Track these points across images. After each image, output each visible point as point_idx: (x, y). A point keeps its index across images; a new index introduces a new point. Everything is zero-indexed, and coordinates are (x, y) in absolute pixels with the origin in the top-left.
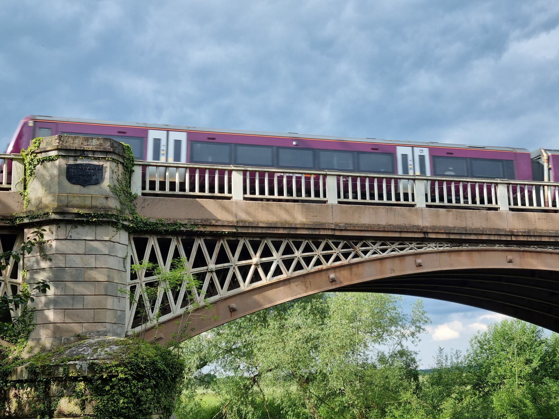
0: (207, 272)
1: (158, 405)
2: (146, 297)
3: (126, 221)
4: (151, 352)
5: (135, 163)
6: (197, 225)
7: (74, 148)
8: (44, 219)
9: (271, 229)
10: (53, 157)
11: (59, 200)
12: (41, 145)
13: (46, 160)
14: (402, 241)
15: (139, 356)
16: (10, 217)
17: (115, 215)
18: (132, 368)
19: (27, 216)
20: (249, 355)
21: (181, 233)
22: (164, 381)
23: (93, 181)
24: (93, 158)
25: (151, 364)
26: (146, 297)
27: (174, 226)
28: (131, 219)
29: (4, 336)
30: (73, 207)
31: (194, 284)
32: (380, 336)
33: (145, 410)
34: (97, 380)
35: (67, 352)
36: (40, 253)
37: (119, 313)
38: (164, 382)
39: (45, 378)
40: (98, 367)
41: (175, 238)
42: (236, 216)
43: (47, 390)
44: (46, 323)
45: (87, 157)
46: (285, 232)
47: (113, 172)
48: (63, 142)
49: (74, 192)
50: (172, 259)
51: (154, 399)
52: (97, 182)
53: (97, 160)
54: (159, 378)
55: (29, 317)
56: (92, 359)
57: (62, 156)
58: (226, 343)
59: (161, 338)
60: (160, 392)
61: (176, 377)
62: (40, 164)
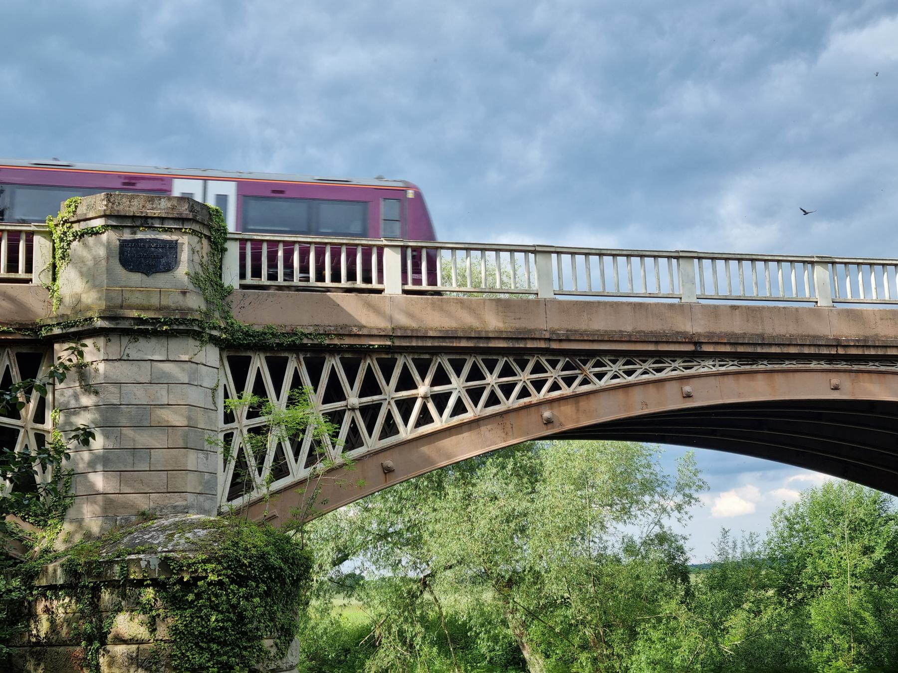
0: (346, 410)
1: (271, 624)
2: (249, 451)
3: (216, 329)
4: (259, 539)
5: (229, 236)
6: (329, 335)
7: (132, 214)
8: (86, 328)
9: (447, 340)
10: (97, 229)
11: (108, 298)
12: (78, 209)
13: (87, 233)
14: (659, 357)
15: (240, 545)
16: (32, 324)
17: (197, 320)
18: (229, 566)
19: (58, 324)
20: (416, 543)
22: (281, 585)
23: (161, 267)
25: (260, 559)
26: (249, 450)
27: (291, 337)
28: (223, 326)
29: (25, 515)
30: (131, 308)
31: (325, 429)
32: (625, 511)
33: (251, 631)
34: (174, 584)
35: (125, 540)
36: (80, 383)
37: (207, 476)
38: (281, 587)
39: (92, 582)
40: (175, 564)
41: (295, 356)
42: (391, 319)
43: (96, 600)
44: (92, 494)
46: (470, 344)
47: (193, 251)
48: (113, 204)
50: (290, 390)
51: (265, 614)
52: (169, 268)
53: (168, 233)
54: (273, 580)
55: (65, 484)
56: (165, 552)
57: (112, 226)
58: (378, 525)
60: (274, 603)
61: (299, 580)
62: (77, 240)
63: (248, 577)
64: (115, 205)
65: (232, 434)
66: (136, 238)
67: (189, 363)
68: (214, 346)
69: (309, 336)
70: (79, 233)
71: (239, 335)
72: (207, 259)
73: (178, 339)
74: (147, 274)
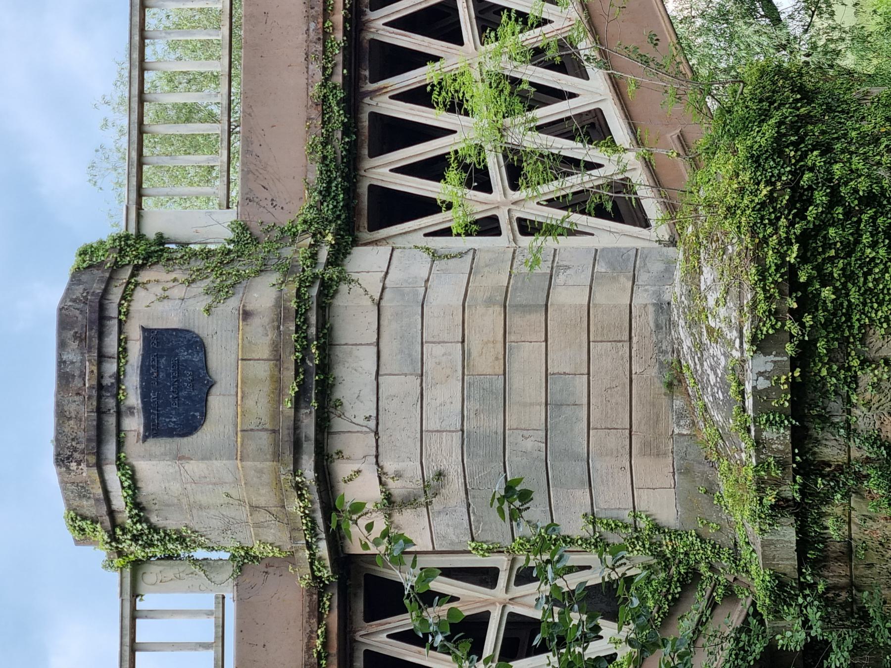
2: (553, 189)
3: (316, 254)
5: (132, 231)
6: (325, 33)
8: (316, 497)
10: (124, 478)
12: (88, 514)
15: (733, 204)
16: (311, 595)
17: (298, 290)
18: (771, 223)
19: (309, 546)
21: (352, 84)
22: (811, 124)
23: (196, 359)
24: (123, 361)
25: (760, 165)
26: (552, 188)
27: (330, 107)
28: (310, 240)
29: (667, 600)
34: (802, 325)
35: (718, 417)
37: (601, 268)
38: (814, 124)
39: (794, 477)
40: (764, 325)
41: (367, 100)
43: (828, 469)
45: (119, 378)
49: (230, 413)
50: (434, 108)
51: (865, 153)
54: (802, 140)
55: (612, 529)
56: (741, 343)
59: (682, 139)
60: (845, 136)
61: (801, 89)
63: (794, 186)
64: (78, 446)
65: (521, 222)
66: (140, 406)
67: (383, 303)
68: (349, 257)
69: (329, 72)
70: (135, 511)
71: (327, 209)
73: (336, 326)
74: (211, 385)
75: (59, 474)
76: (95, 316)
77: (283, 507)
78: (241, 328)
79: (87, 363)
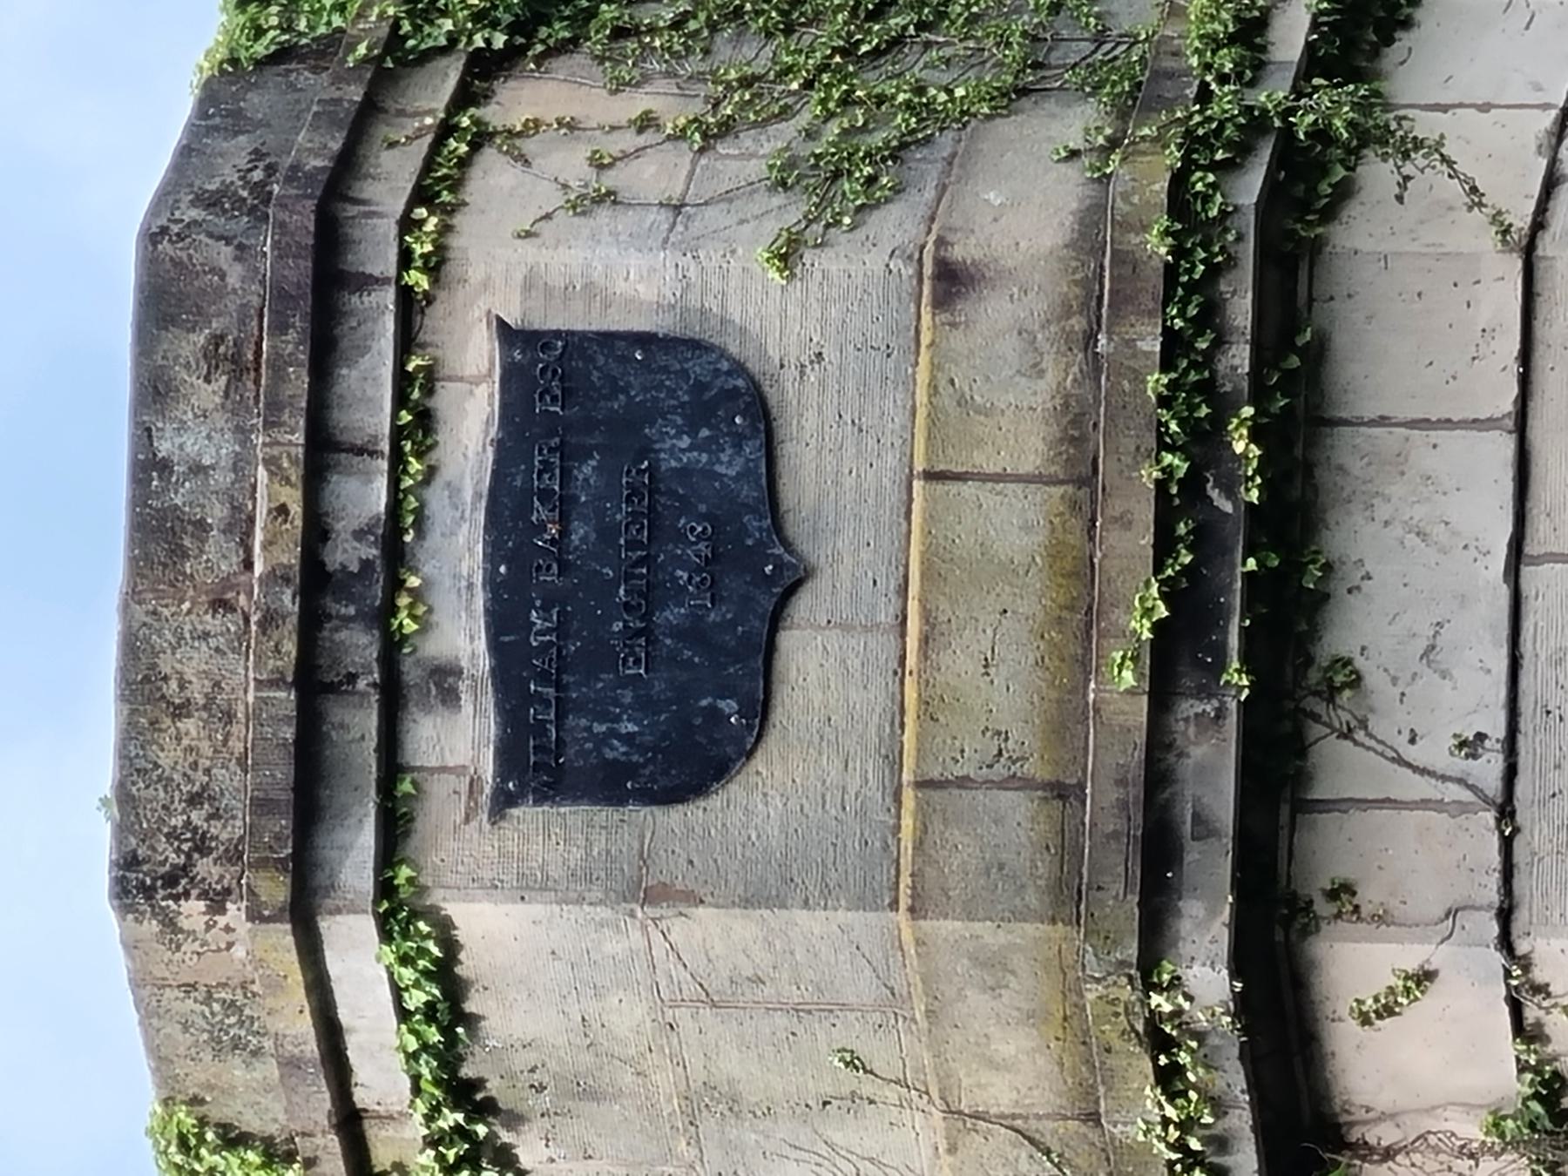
7: (286, 698)
8: (1233, 1080)
10: (408, 975)
12: (251, 1122)
13: (448, 1057)
17: (1179, 180)
23: (728, 466)
24: (415, 466)
48: (202, 846)
49: (871, 700)
62: (506, 1137)
64: (215, 828)
66: (484, 663)
67: (1547, 246)
68: (1404, 39)
70: (451, 1118)
72: (661, 85)
73: (1341, 342)
75: (131, 946)
76: (300, 270)
77: (1093, 1118)
78: (925, 339)
79: (262, 473)
